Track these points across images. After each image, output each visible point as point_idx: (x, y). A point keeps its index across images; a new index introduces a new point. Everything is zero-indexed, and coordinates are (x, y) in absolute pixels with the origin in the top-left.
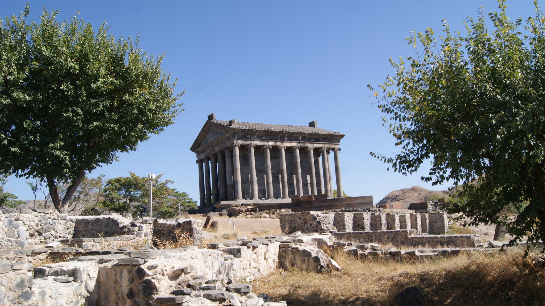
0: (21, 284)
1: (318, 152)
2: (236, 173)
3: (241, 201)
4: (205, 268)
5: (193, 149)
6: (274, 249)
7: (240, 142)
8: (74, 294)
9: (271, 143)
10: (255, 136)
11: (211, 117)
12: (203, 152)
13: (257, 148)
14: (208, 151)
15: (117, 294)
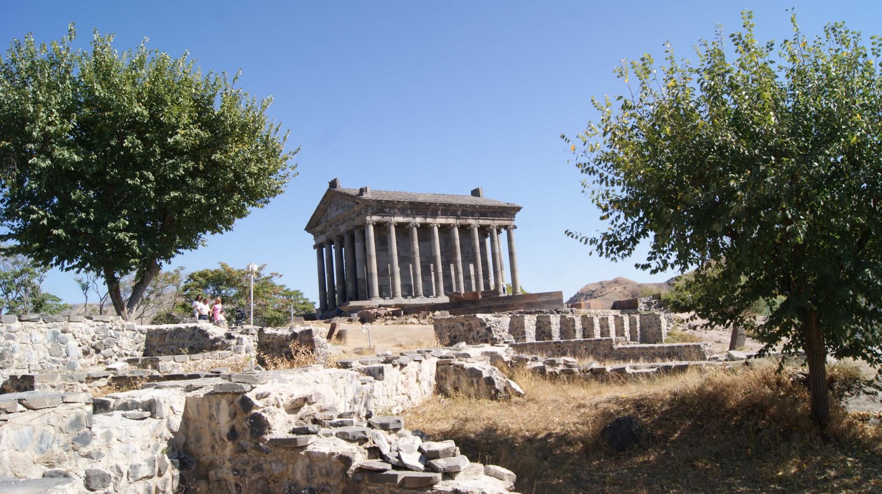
0: (76, 423)
1: (484, 231)
2: (370, 262)
3: (377, 301)
4: (334, 395)
5: (309, 228)
6: (429, 367)
7: (376, 218)
8: (152, 436)
9: (419, 220)
10: (396, 210)
11: (333, 184)
12: (322, 233)
13: (400, 227)
14: (331, 232)
15: (213, 434)
